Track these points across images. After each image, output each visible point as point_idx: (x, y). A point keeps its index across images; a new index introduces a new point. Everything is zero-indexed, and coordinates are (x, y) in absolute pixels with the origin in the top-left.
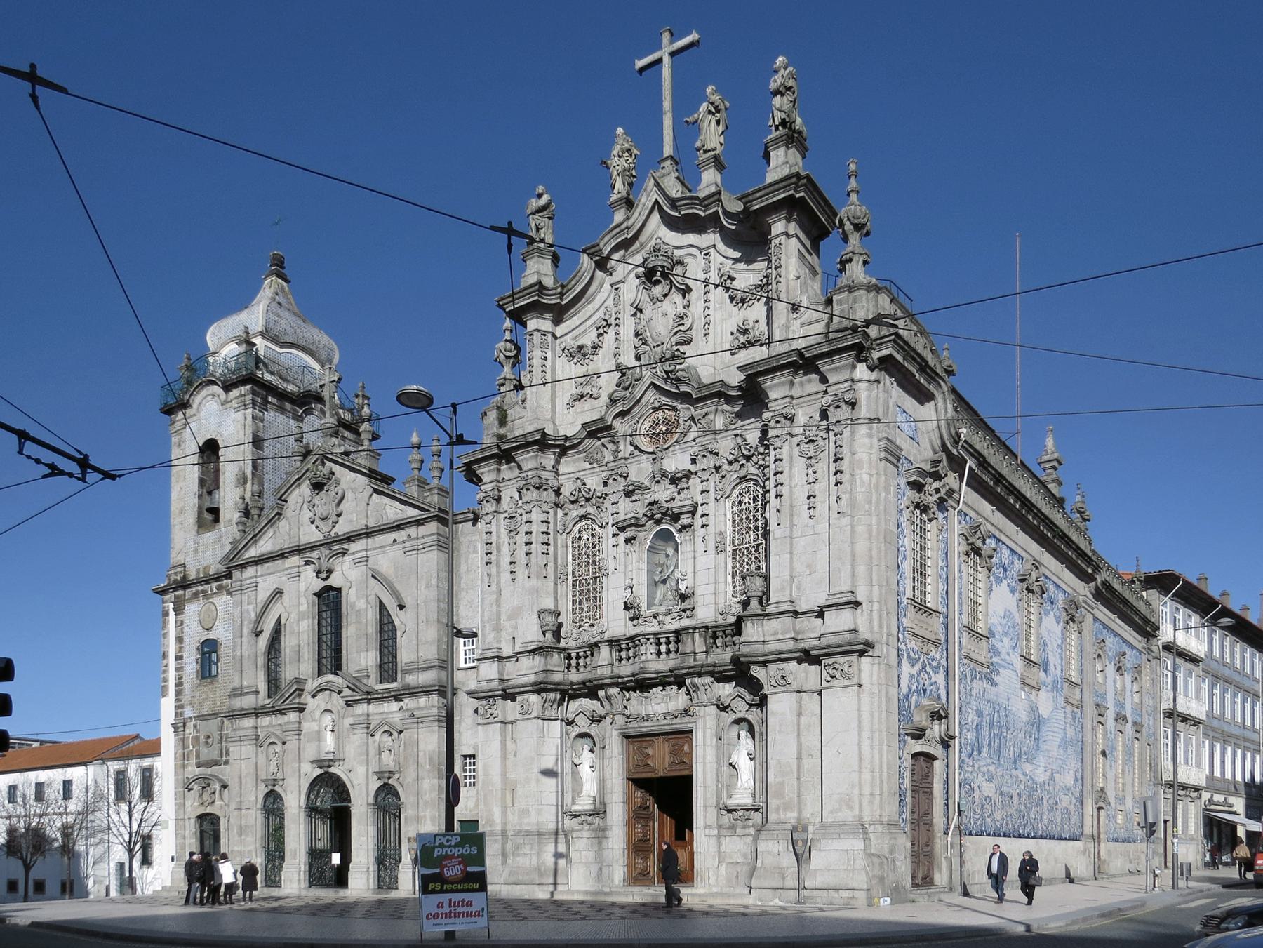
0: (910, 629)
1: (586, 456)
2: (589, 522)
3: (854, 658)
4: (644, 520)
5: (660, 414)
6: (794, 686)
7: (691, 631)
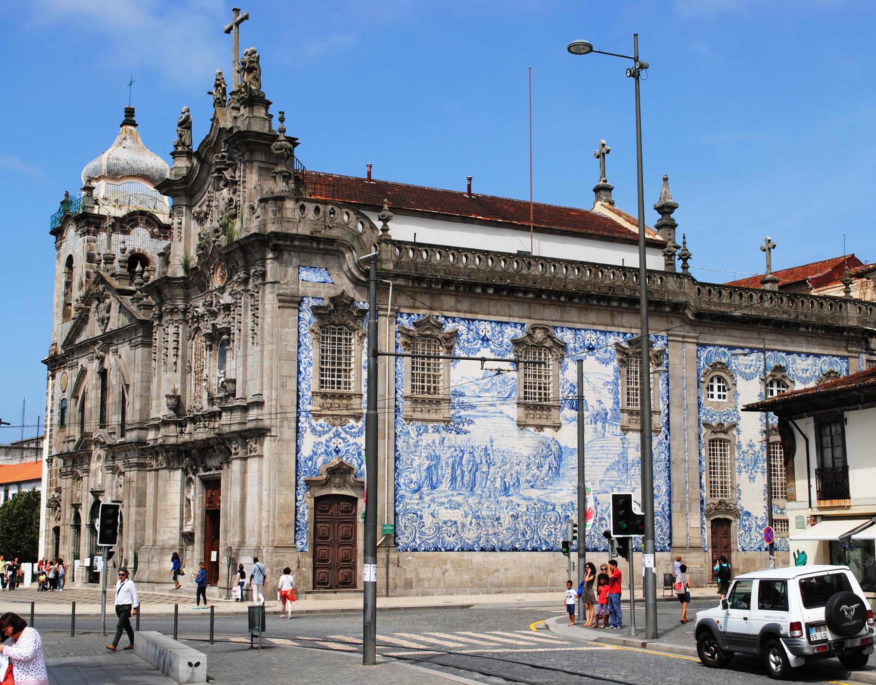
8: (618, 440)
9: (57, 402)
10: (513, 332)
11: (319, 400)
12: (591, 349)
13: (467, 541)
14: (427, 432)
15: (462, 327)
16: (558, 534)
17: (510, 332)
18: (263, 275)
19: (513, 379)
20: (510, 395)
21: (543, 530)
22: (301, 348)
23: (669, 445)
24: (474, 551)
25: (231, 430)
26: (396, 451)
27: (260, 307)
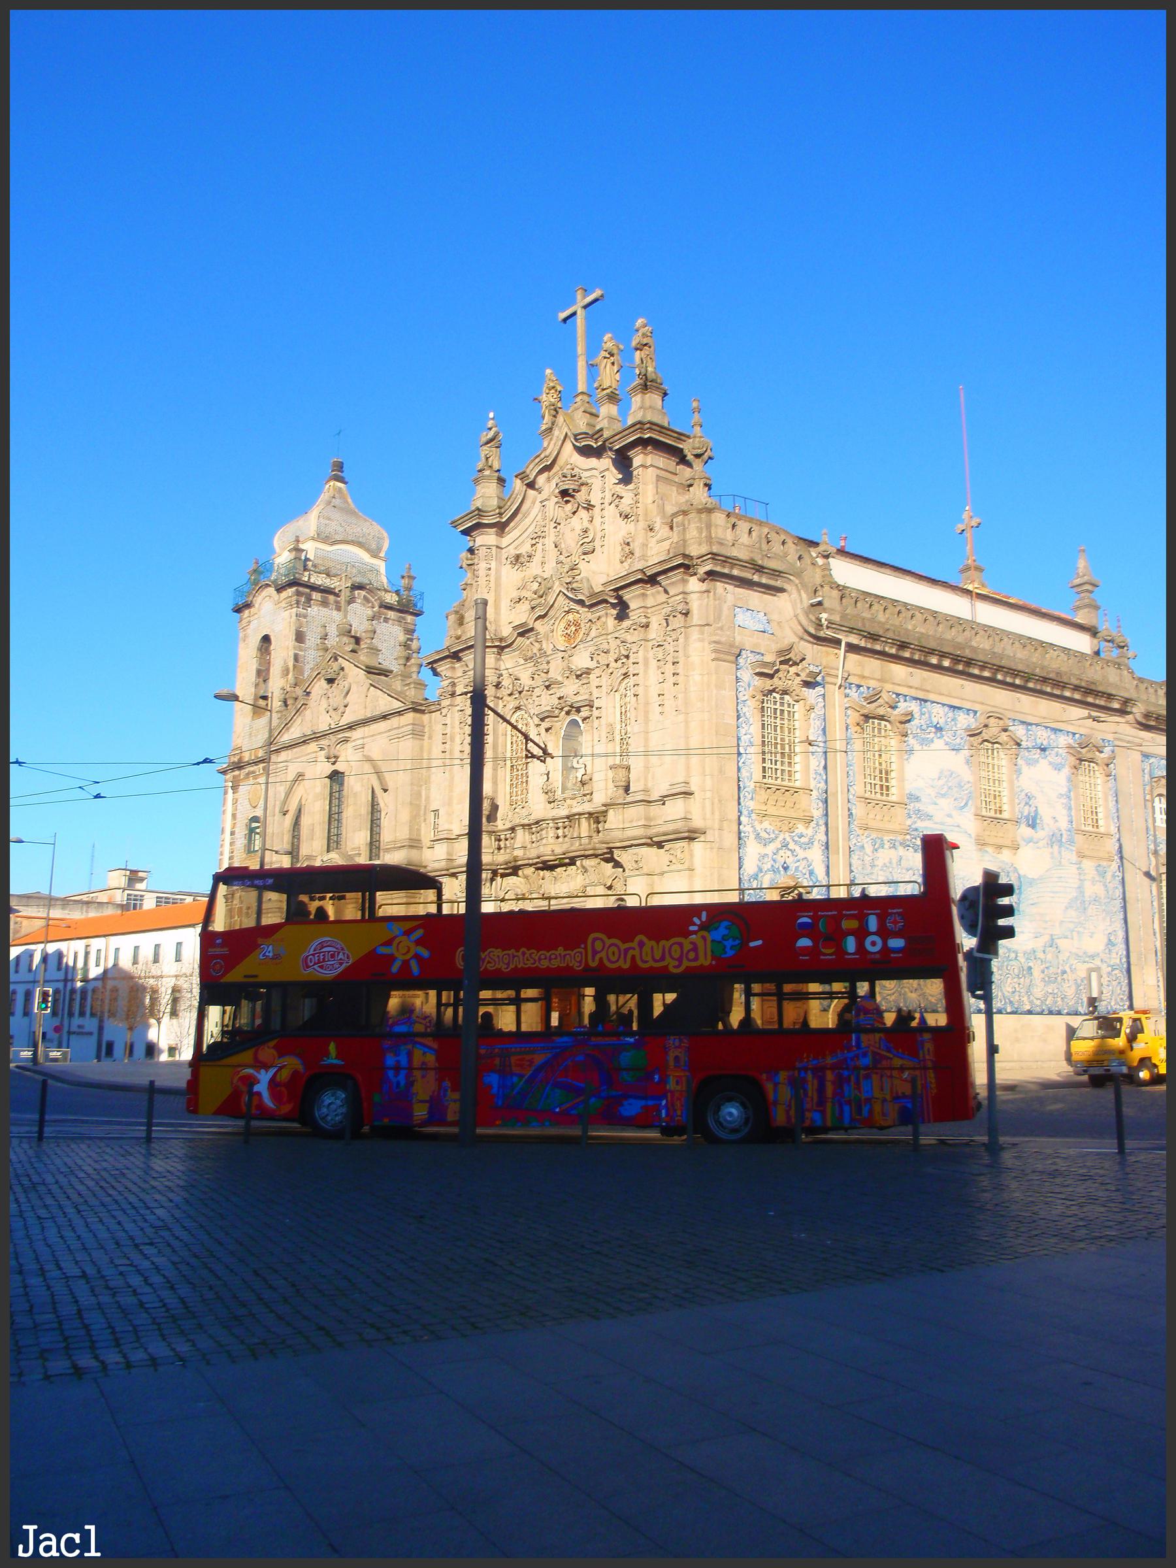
0: (757, 812)
1: (521, 653)
2: (523, 712)
3: (684, 843)
4: (557, 711)
5: (570, 617)
6: (645, 870)
7: (577, 817)
8: (1074, 869)
9: (242, 821)
10: (966, 721)
11: (763, 795)
12: (1043, 750)
13: (930, 998)
14: (883, 847)
15: (914, 707)
16: (1022, 991)
17: (965, 721)
18: (686, 614)
19: (969, 782)
20: (966, 804)
21: (1007, 985)
22: (740, 720)
23: (1123, 879)
24: (937, 1012)
25: (625, 836)
26: (851, 871)
27: (681, 660)
